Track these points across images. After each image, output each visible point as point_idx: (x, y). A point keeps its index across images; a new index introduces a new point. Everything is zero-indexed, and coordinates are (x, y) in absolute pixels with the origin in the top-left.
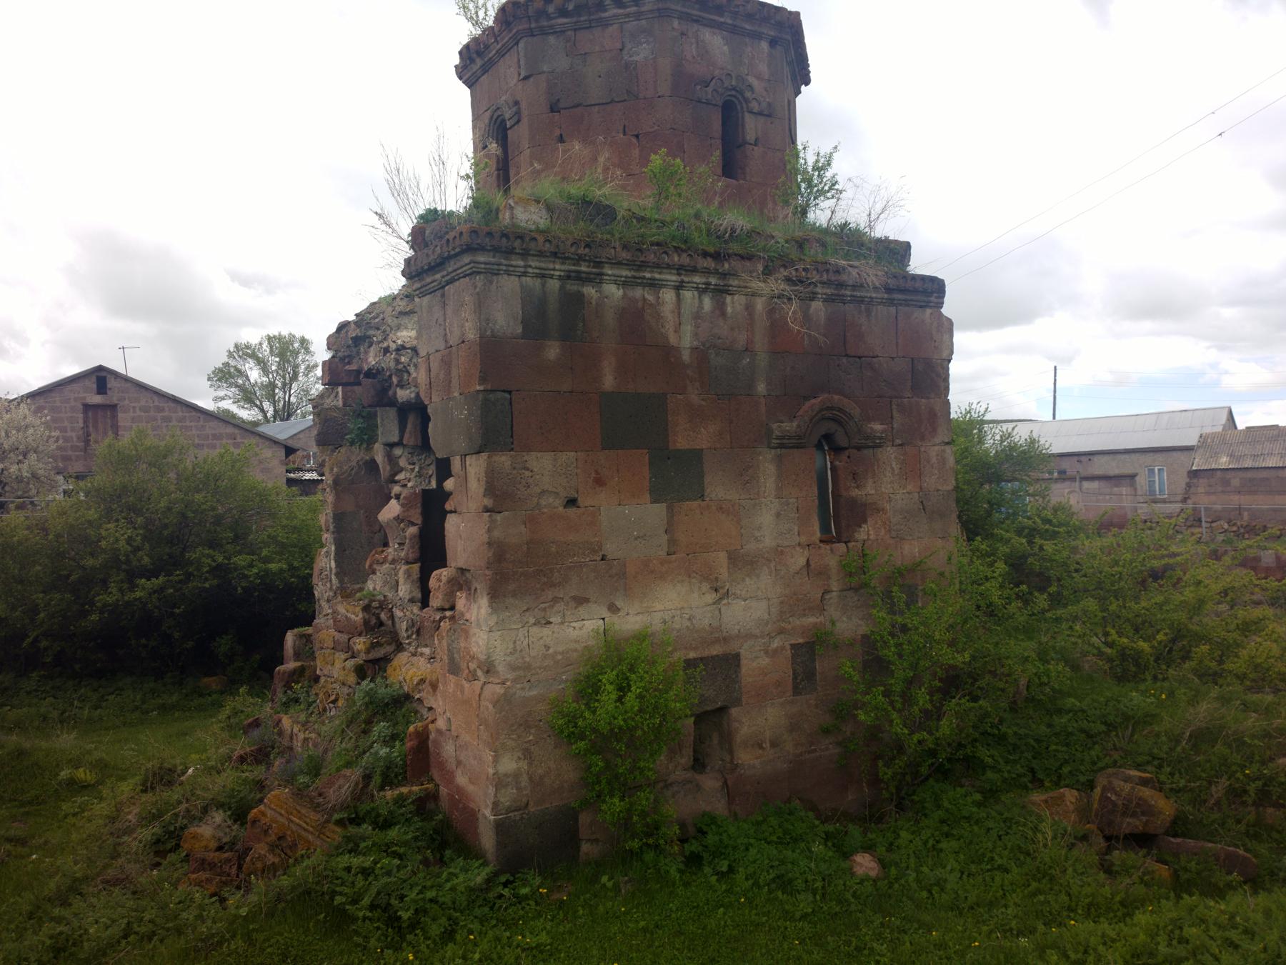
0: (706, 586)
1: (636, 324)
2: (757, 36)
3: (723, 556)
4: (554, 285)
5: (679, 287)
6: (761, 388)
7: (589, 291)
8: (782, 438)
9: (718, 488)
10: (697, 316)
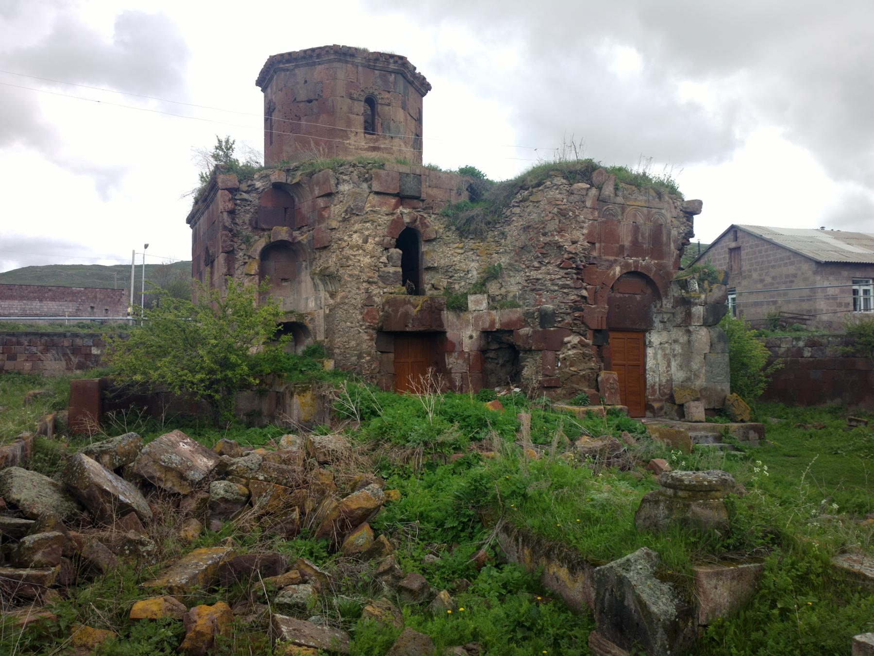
2: (272, 77)
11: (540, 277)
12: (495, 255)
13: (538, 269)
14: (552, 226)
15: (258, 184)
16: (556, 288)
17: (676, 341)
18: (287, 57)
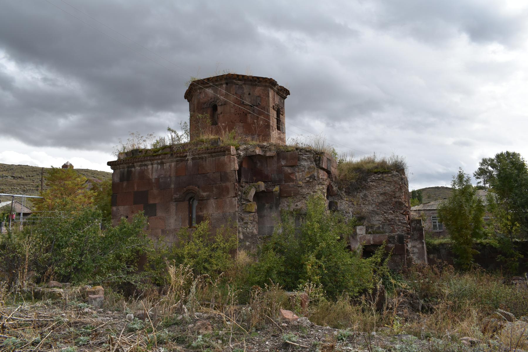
0: (155, 238)
1: (142, 175)
3: (160, 230)
4: (126, 169)
5: (152, 164)
6: (173, 186)
7: (133, 169)
8: (176, 199)
9: (159, 213)
10: (157, 170)
11: (393, 218)
12: (362, 205)
13: (392, 214)
14: (397, 194)
15: (242, 153)
16: (400, 224)
17: (414, 247)
18: (241, 77)
